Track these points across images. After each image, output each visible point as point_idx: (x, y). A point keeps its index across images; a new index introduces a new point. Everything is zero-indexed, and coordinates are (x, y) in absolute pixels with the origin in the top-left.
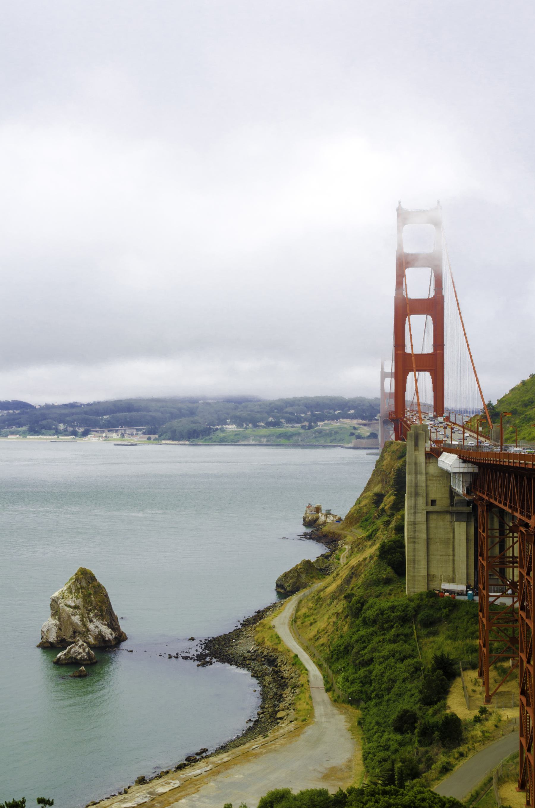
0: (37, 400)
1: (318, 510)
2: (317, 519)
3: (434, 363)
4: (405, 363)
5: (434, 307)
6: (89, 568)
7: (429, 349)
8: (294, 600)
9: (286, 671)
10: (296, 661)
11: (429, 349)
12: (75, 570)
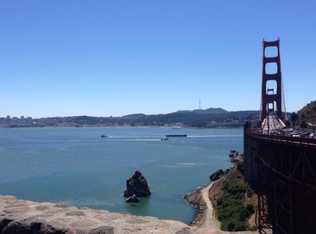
0: (35, 116)
1: (234, 151)
2: (233, 155)
3: (278, 98)
4: (266, 99)
5: (277, 77)
6: (140, 171)
7: (275, 93)
8: (213, 183)
9: (201, 208)
10: (205, 205)
11: (275, 93)
12: (135, 171)
